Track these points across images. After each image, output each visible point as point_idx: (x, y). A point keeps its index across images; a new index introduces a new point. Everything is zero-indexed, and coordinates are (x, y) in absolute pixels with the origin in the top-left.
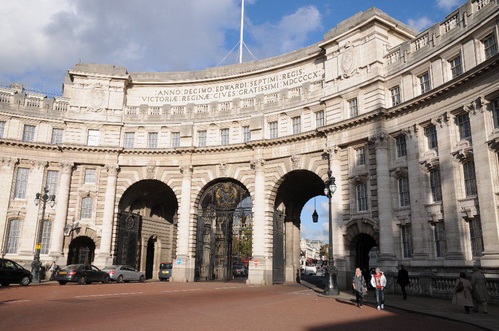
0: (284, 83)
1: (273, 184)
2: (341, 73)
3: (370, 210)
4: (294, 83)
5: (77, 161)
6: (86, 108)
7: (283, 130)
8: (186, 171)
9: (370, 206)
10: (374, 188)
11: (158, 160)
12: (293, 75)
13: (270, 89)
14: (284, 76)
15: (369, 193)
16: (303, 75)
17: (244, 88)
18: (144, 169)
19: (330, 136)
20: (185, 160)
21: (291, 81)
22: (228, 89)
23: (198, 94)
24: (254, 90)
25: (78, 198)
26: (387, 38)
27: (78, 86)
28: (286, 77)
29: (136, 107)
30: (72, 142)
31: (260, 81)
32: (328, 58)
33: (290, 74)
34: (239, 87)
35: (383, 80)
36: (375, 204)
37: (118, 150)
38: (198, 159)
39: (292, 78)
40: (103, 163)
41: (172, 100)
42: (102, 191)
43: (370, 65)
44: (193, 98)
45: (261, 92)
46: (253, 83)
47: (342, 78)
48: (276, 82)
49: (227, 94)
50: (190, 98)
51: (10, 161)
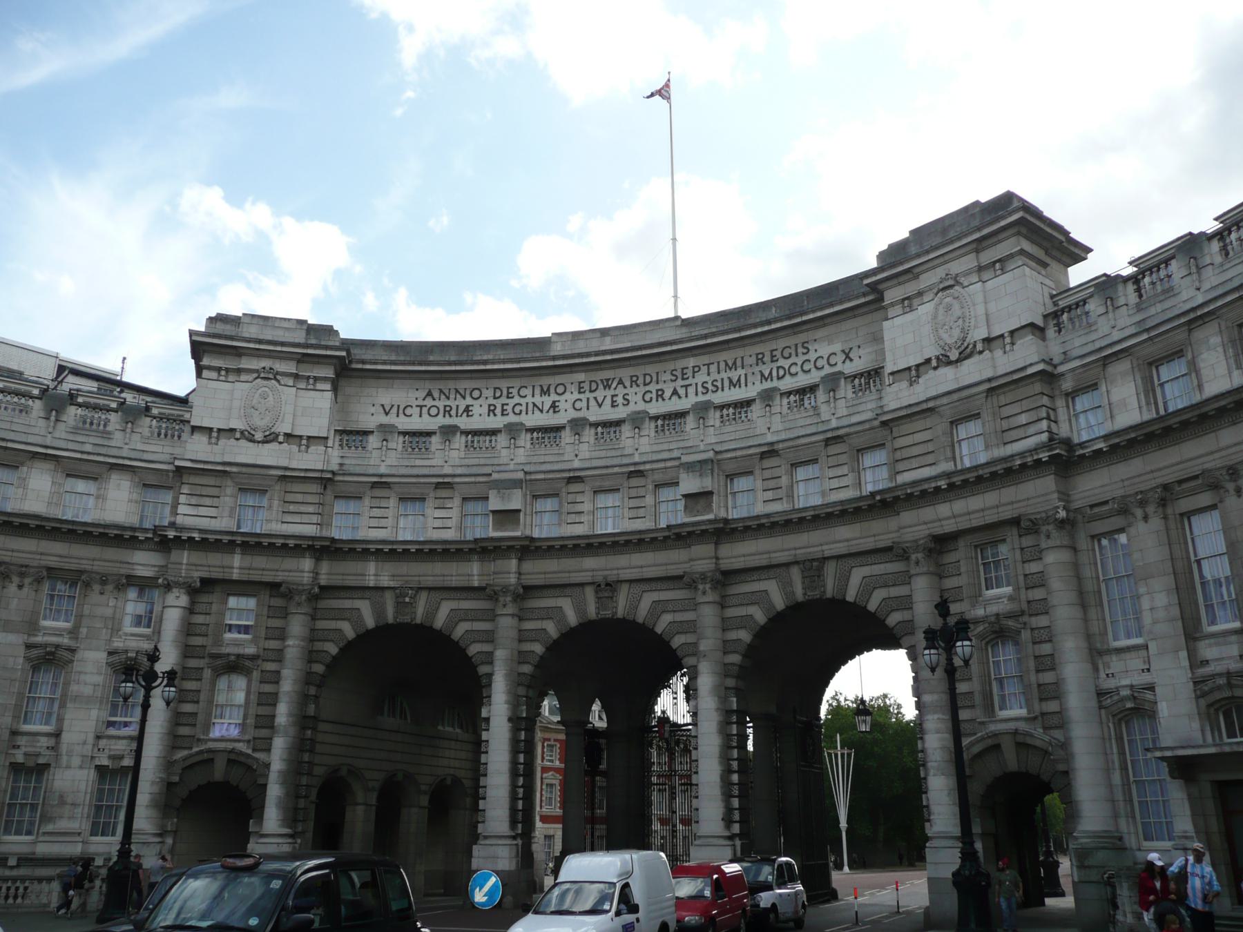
0: (762, 375)
2: (932, 352)
4: (787, 376)
5: (205, 575)
6: (232, 430)
10: (1046, 649)
12: (787, 355)
13: (726, 389)
14: (760, 356)
16: (812, 356)
17: (653, 387)
19: (907, 517)
21: (781, 372)
22: (610, 388)
23: (529, 399)
24: (682, 392)
25: (207, 673)
26: (1045, 265)
27: (214, 375)
28: (767, 358)
29: (366, 433)
31: (696, 369)
32: (891, 312)
33: (778, 353)
34: (640, 381)
35: (1049, 368)
36: (1051, 692)
37: (318, 544)
39: (782, 362)
40: (278, 579)
41: (460, 412)
43: (1012, 333)
44: (517, 410)
45: (701, 398)
46: (678, 373)
47: (934, 363)
48: (741, 372)
49: (608, 401)
50: (509, 408)
51: (22, 575)
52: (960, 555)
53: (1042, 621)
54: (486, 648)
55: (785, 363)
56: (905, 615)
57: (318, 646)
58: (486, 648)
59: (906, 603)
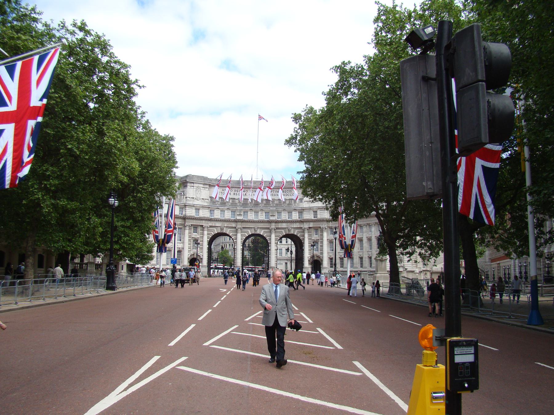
1: (279, 238)
3: (319, 252)
6: (193, 198)
7: (284, 216)
8: (240, 230)
9: (319, 250)
10: (321, 244)
11: (226, 224)
15: (319, 246)
18: (219, 228)
20: (239, 225)
25: (192, 241)
30: (189, 214)
33: (286, 191)
36: (322, 250)
37: (209, 219)
38: (245, 225)
39: (287, 193)
42: (201, 237)
50: (237, 194)
52: (312, 230)
53: (322, 240)
54: (235, 237)
55: (288, 193)
56: (303, 237)
57: (208, 236)
58: (235, 237)
59: (304, 236)
